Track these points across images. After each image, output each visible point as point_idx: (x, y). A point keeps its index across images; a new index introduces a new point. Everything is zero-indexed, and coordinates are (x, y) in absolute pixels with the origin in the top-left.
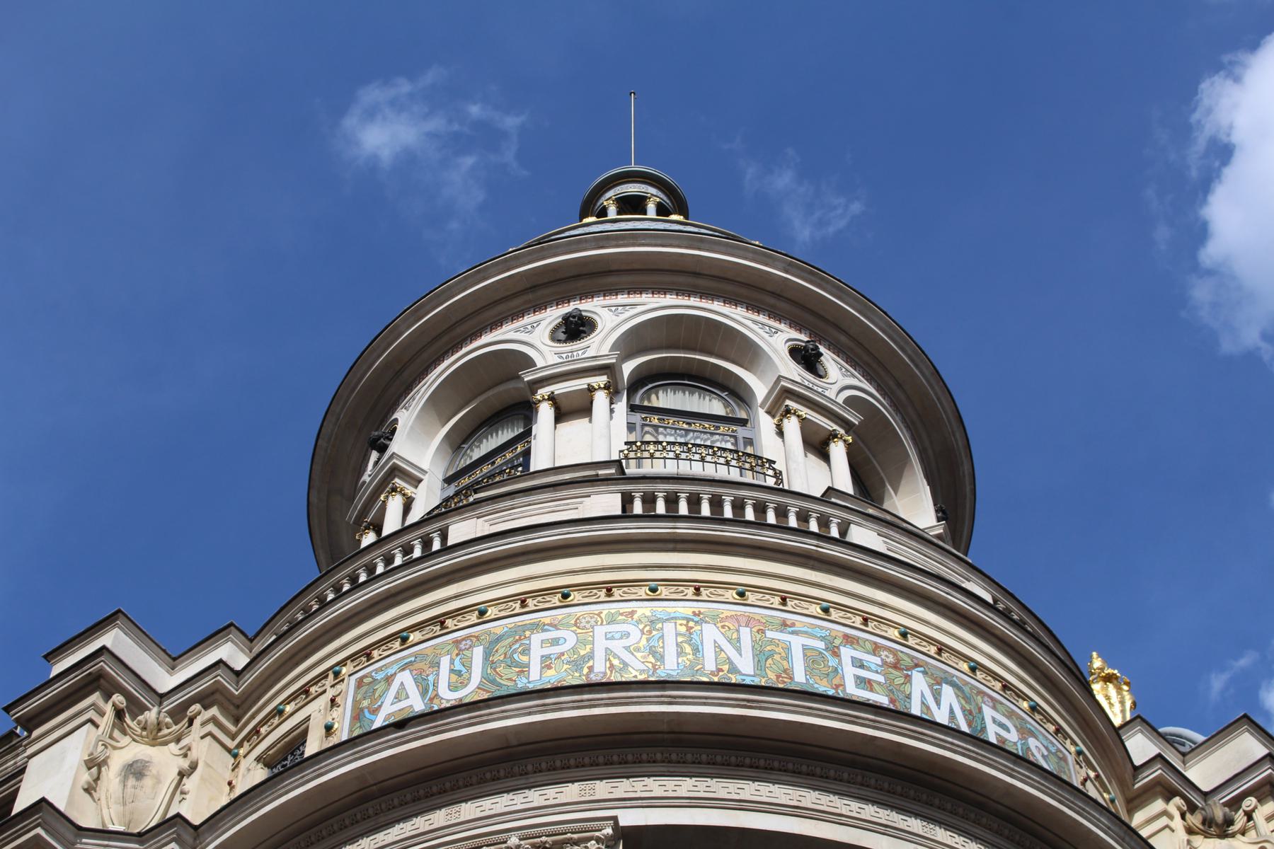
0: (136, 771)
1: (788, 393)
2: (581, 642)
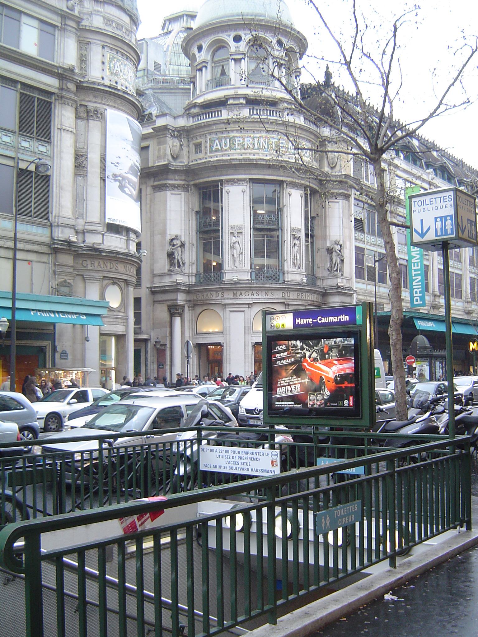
2: (244, 141)
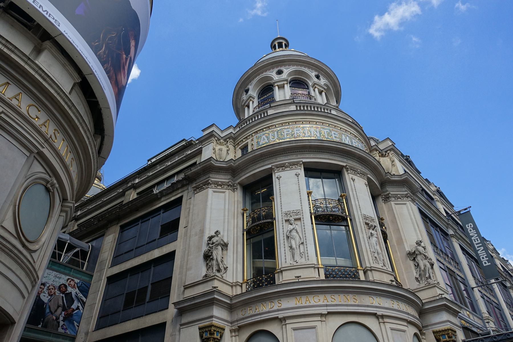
0: (221, 150)
1: (315, 84)
2: (292, 131)
